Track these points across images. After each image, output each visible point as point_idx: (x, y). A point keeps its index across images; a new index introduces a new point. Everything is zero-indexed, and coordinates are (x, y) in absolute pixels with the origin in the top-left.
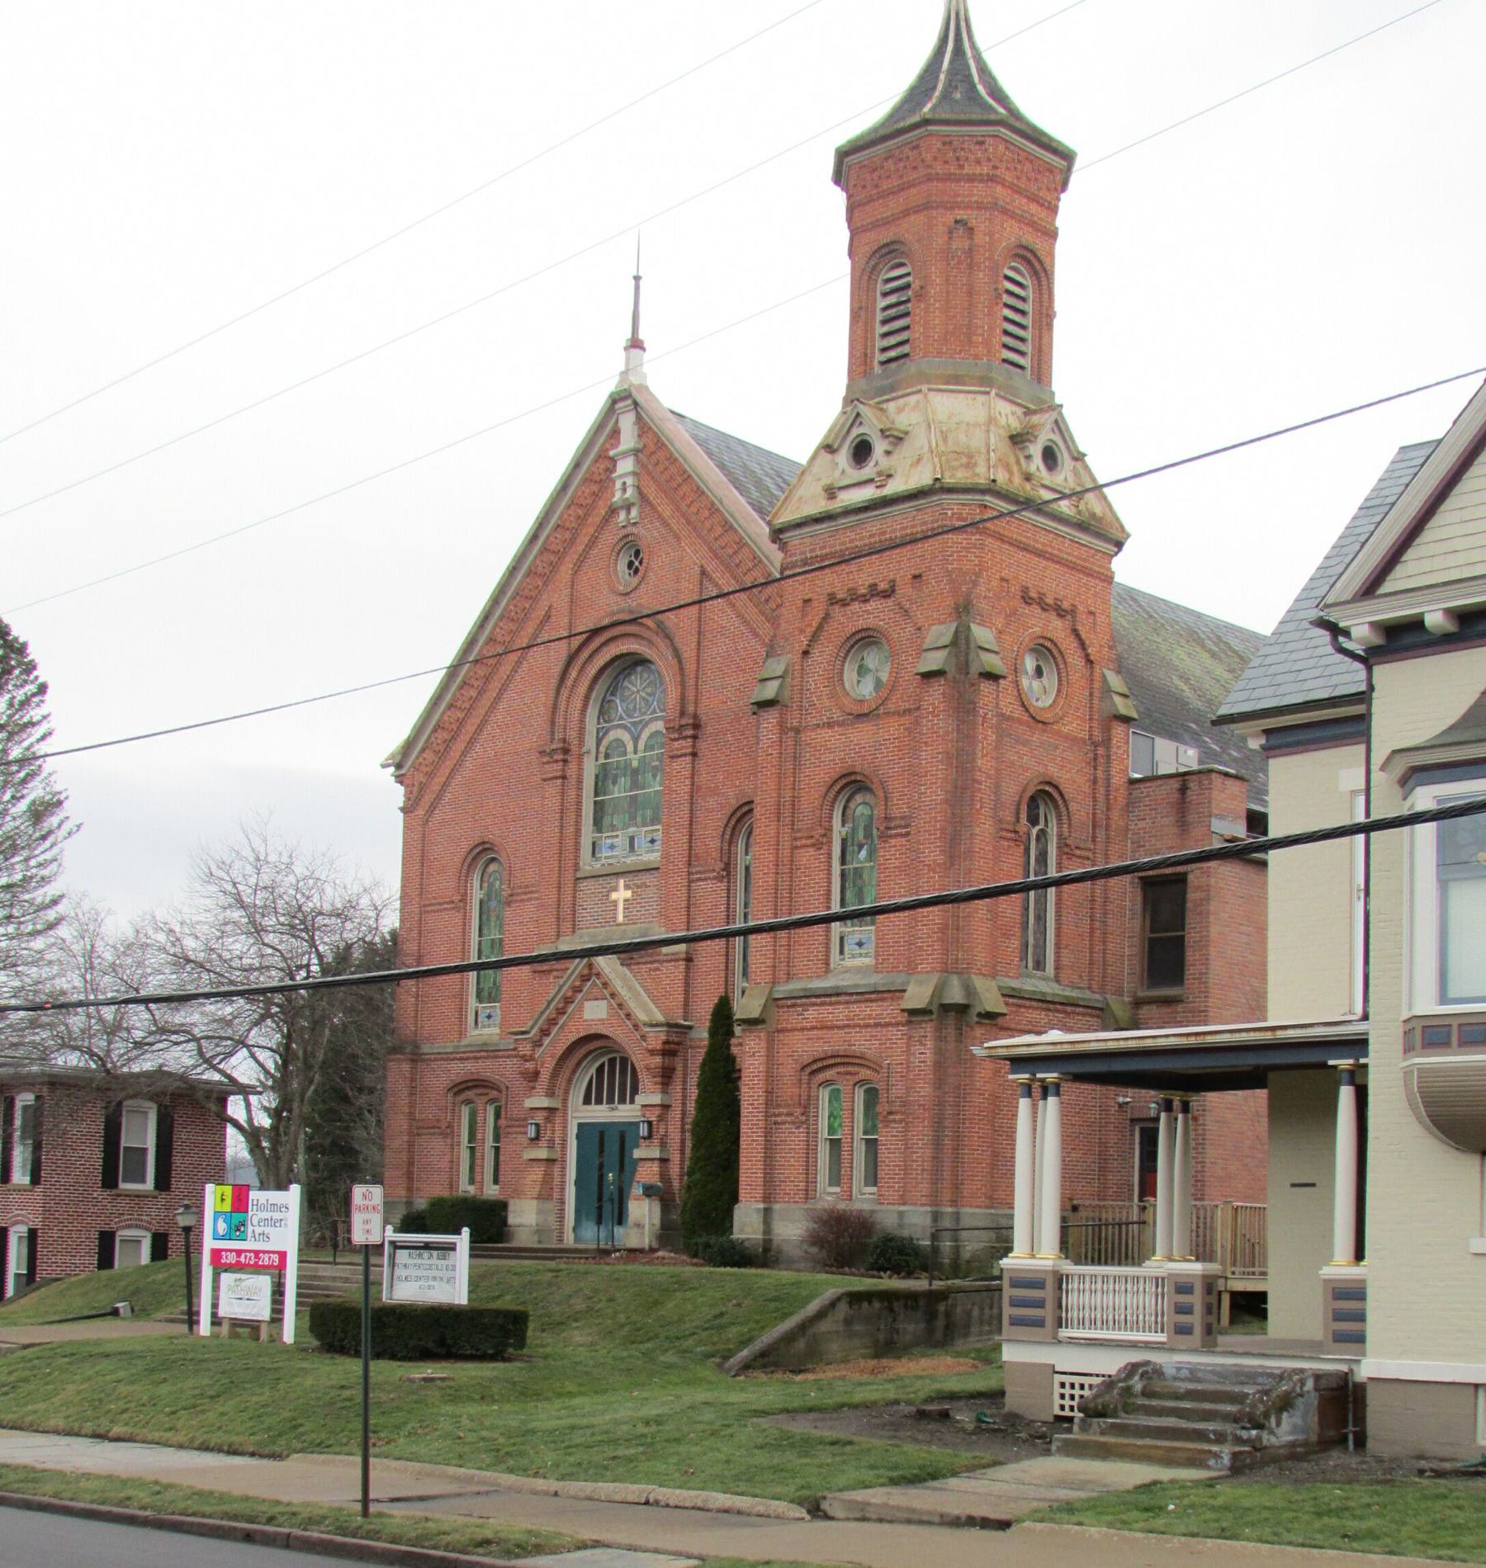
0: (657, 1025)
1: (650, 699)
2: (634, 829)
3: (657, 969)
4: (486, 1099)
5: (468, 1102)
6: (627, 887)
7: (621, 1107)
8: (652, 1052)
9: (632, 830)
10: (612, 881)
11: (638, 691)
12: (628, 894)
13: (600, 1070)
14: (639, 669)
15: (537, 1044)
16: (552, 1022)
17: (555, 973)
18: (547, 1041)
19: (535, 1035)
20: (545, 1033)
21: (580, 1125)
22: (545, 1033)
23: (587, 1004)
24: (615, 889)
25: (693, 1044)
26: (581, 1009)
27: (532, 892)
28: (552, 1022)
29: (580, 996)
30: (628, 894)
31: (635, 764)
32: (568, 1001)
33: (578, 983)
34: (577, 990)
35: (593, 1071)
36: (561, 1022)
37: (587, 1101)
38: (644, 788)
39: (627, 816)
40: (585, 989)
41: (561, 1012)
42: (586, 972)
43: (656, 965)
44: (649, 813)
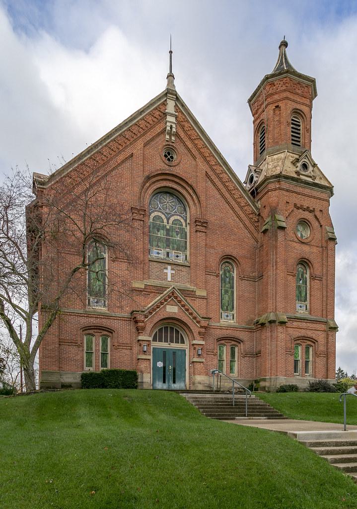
1: (174, 207)
6: (172, 269)
8: (202, 327)
9: (168, 250)
10: (166, 265)
11: (168, 202)
13: (160, 330)
14: (168, 195)
23: (168, 307)
26: (165, 307)
30: (174, 272)
31: (168, 227)
33: (167, 298)
39: (165, 245)
42: (171, 295)
43: (194, 298)
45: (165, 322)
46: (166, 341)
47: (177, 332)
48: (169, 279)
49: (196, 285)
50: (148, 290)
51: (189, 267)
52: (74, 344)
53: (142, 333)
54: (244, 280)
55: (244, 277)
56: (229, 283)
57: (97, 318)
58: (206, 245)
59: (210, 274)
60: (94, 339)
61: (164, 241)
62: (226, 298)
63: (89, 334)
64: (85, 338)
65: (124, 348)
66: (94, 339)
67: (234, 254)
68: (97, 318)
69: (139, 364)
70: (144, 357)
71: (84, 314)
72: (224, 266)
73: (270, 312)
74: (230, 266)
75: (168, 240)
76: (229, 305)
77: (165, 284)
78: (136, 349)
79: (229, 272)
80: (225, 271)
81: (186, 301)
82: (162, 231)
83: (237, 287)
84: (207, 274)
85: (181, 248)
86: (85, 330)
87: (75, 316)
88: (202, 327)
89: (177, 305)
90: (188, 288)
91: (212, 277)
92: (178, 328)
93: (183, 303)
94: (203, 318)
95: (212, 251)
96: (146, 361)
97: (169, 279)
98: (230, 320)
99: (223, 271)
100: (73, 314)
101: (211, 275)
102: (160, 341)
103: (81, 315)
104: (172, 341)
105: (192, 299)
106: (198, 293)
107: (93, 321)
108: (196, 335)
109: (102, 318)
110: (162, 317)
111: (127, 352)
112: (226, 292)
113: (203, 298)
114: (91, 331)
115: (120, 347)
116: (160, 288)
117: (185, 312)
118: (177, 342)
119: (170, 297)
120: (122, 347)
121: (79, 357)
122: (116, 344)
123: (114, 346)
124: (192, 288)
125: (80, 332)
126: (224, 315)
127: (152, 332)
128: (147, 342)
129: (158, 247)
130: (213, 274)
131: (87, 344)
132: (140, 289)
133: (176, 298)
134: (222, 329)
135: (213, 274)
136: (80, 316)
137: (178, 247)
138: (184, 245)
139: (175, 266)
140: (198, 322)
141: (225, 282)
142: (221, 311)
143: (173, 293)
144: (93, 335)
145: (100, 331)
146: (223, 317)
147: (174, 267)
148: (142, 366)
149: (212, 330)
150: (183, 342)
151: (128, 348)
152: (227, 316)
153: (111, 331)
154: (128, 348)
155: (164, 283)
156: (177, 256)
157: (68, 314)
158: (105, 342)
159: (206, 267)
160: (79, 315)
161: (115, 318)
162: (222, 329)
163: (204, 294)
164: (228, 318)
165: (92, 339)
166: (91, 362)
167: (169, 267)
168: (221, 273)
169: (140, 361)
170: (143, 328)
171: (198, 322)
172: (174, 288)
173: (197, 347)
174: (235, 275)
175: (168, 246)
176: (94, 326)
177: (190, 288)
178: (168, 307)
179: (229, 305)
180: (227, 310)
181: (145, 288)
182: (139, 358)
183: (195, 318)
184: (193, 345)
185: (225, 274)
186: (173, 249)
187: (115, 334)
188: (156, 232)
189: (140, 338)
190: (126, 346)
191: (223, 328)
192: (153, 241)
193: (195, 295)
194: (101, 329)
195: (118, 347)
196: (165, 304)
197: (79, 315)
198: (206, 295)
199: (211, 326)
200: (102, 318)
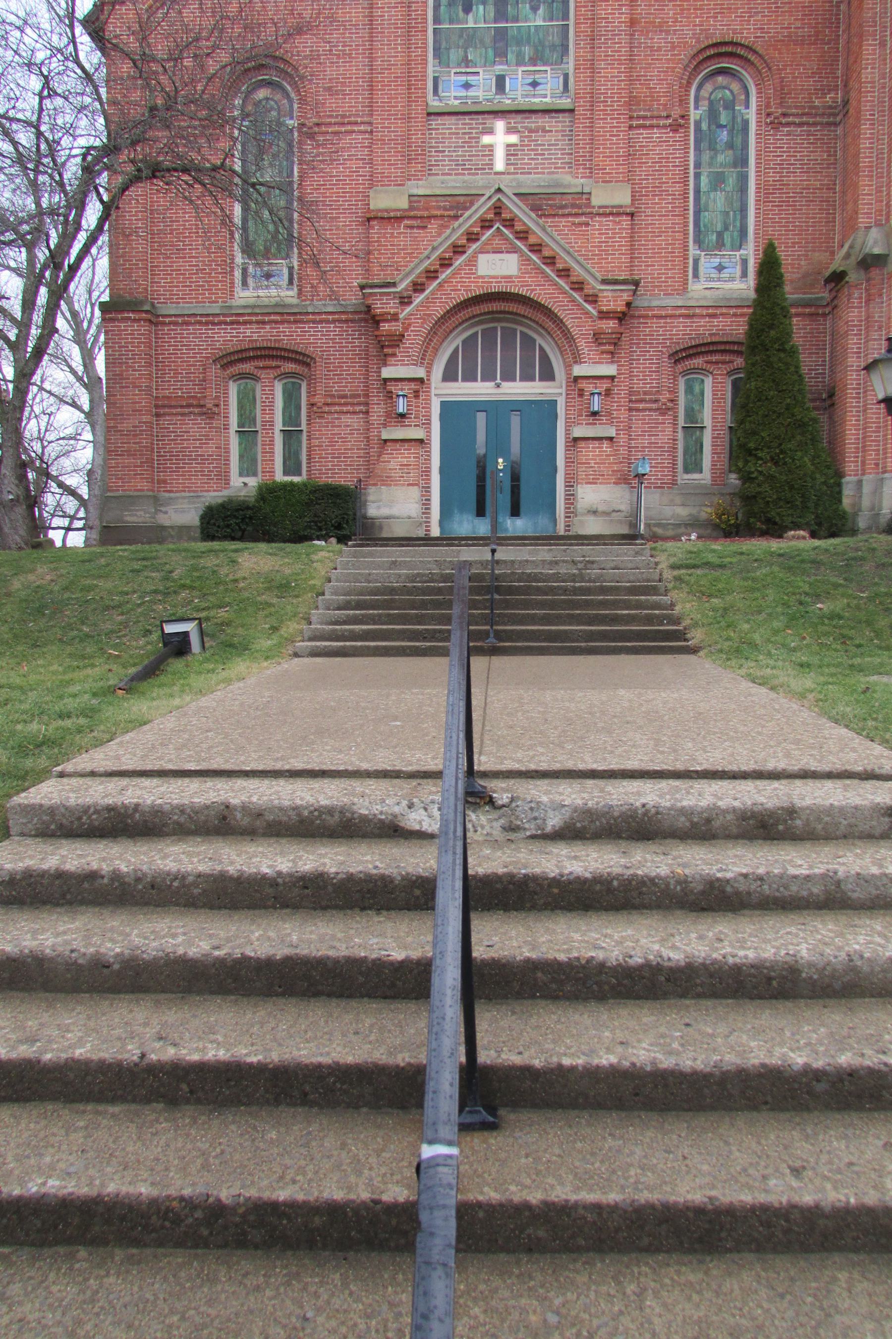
0: (616, 282)
2: (506, 67)
3: (587, 225)
4: (272, 374)
5: (240, 376)
6: (510, 131)
7: (505, 384)
8: (604, 315)
9: (500, 69)
10: (489, 120)
12: (513, 139)
13: (468, 344)
15: (405, 301)
16: (431, 275)
17: (406, 222)
18: (419, 299)
19: (406, 289)
20: (418, 287)
21: (443, 404)
22: (418, 287)
23: (482, 259)
24: (491, 131)
25: (637, 313)
26: (472, 262)
27: (356, 123)
28: (431, 275)
29: (474, 246)
30: (513, 139)
32: (458, 250)
33: (476, 230)
34: (472, 237)
35: (458, 342)
36: (442, 277)
37: (449, 375)
38: (517, 21)
39: (491, 53)
40: (484, 238)
41: (445, 263)
42: (490, 216)
43: (583, 219)
44: (527, 51)
45: (477, 310)
46: (489, 376)
47: (527, 343)
48: (500, 165)
49: (591, 173)
50: (419, 213)
51: (572, 111)
52: (196, 410)
53: (394, 355)
54: (788, 124)
55: (784, 115)
56: (730, 146)
57: (264, 323)
58: (633, 22)
59: (648, 123)
60: (258, 387)
61: (488, 41)
62: (718, 201)
63: (241, 376)
64: (233, 389)
65: (345, 409)
66: (258, 387)
67: (747, 33)
68: (264, 323)
69: (385, 457)
70: (399, 433)
71: (225, 315)
72: (709, 87)
73: (868, 228)
74: (735, 86)
75: (501, 34)
76: (726, 228)
77: (480, 184)
78: (378, 411)
79: (730, 106)
80: (711, 103)
81: (544, 229)
82: (481, 8)
83: (758, 157)
84: (639, 127)
85: (547, 51)
86: (231, 363)
87: (200, 323)
88: (604, 315)
89: (514, 250)
90: (565, 187)
91: (656, 134)
92: (530, 327)
93: (532, 240)
94: (604, 282)
95: (658, 40)
96: (406, 445)
97: (500, 165)
98: (732, 279)
99: (704, 106)
100: (193, 320)
101: (652, 127)
102: (470, 377)
103: (216, 320)
104: (509, 376)
105: (577, 220)
106: (601, 197)
107: (252, 334)
108: (583, 345)
109: (276, 322)
110: (463, 295)
111: (355, 421)
112: (718, 181)
113: (614, 212)
114: (247, 367)
115: (333, 409)
116: (462, 199)
117: (543, 272)
118: (528, 377)
119: (486, 224)
120: (337, 408)
121: (211, 449)
122: (319, 400)
123: (313, 405)
124: (573, 182)
125: (214, 371)
126: (707, 264)
127: (436, 350)
128: (413, 386)
129: (466, 62)
130: (661, 123)
131: (241, 407)
132: (392, 214)
133: (510, 223)
134: (694, 316)
135: (661, 123)
136: (214, 324)
137: (536, 51)
138: (557, 41)
139: (519, 118)
140: (592, 299)
141: (712, 148)
142: (693, 251)
143: (498, 209)
144: (256, 379)
145: (274, 363)
146: (702, 270)
147: (515, 120)
148: (393, 464)
149: (654, 324)
150: (548, 375)
151: (358, 408)
152: (720, 268)
153: (303, 359)
154: (358, 408)
155: (479, 181)
156: (534, 84)
157: (180, 320)
158: (291, 397)
159: (632, 101)
160: (209, 321)
161: (318, 318)
162: (694, 316)
163: (622, 197)
164: (725, 274)
165: (254, 391)
166: (254, 461)
167: (500, 125)
168: (694, 115)
169: (390, 447)
170: (397, 340)
171: (592, 299)
172: (499, 190)
173: (589, 387)
174: (752, 115)
175: (501, 54)
176: (254, 349)
177: (569, 186)
178: (482, 259)
179: (726, 228)
180: (720, 245)
181: (411, 208)
182: (384, 437)
183: (578, 286)
184: (576, 379)
185: (713, 114)
186: (519, 64)
187: (320, 370)
188: (461, 14)
189: (386, 373)
190: (353, 404)
191: (697, 311)
192: (448, 49)
193: (589, 205)
194: (272, 357)
195: (326, 409)
196: (470, 252)
197: (209, 321)
198: (627, 200)
199: (650, 308)
200: (276, 322)
